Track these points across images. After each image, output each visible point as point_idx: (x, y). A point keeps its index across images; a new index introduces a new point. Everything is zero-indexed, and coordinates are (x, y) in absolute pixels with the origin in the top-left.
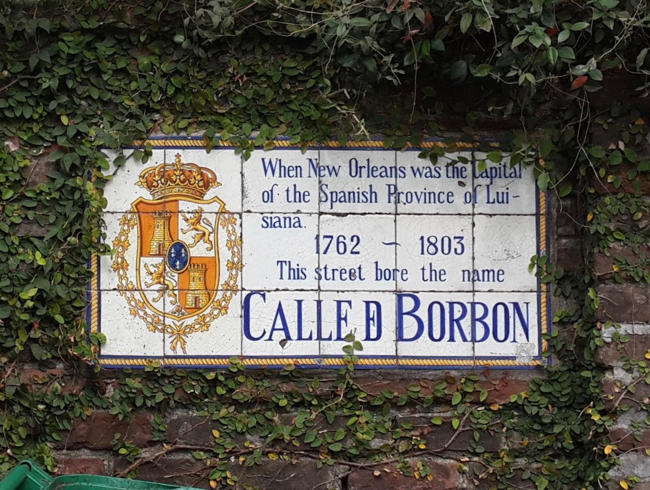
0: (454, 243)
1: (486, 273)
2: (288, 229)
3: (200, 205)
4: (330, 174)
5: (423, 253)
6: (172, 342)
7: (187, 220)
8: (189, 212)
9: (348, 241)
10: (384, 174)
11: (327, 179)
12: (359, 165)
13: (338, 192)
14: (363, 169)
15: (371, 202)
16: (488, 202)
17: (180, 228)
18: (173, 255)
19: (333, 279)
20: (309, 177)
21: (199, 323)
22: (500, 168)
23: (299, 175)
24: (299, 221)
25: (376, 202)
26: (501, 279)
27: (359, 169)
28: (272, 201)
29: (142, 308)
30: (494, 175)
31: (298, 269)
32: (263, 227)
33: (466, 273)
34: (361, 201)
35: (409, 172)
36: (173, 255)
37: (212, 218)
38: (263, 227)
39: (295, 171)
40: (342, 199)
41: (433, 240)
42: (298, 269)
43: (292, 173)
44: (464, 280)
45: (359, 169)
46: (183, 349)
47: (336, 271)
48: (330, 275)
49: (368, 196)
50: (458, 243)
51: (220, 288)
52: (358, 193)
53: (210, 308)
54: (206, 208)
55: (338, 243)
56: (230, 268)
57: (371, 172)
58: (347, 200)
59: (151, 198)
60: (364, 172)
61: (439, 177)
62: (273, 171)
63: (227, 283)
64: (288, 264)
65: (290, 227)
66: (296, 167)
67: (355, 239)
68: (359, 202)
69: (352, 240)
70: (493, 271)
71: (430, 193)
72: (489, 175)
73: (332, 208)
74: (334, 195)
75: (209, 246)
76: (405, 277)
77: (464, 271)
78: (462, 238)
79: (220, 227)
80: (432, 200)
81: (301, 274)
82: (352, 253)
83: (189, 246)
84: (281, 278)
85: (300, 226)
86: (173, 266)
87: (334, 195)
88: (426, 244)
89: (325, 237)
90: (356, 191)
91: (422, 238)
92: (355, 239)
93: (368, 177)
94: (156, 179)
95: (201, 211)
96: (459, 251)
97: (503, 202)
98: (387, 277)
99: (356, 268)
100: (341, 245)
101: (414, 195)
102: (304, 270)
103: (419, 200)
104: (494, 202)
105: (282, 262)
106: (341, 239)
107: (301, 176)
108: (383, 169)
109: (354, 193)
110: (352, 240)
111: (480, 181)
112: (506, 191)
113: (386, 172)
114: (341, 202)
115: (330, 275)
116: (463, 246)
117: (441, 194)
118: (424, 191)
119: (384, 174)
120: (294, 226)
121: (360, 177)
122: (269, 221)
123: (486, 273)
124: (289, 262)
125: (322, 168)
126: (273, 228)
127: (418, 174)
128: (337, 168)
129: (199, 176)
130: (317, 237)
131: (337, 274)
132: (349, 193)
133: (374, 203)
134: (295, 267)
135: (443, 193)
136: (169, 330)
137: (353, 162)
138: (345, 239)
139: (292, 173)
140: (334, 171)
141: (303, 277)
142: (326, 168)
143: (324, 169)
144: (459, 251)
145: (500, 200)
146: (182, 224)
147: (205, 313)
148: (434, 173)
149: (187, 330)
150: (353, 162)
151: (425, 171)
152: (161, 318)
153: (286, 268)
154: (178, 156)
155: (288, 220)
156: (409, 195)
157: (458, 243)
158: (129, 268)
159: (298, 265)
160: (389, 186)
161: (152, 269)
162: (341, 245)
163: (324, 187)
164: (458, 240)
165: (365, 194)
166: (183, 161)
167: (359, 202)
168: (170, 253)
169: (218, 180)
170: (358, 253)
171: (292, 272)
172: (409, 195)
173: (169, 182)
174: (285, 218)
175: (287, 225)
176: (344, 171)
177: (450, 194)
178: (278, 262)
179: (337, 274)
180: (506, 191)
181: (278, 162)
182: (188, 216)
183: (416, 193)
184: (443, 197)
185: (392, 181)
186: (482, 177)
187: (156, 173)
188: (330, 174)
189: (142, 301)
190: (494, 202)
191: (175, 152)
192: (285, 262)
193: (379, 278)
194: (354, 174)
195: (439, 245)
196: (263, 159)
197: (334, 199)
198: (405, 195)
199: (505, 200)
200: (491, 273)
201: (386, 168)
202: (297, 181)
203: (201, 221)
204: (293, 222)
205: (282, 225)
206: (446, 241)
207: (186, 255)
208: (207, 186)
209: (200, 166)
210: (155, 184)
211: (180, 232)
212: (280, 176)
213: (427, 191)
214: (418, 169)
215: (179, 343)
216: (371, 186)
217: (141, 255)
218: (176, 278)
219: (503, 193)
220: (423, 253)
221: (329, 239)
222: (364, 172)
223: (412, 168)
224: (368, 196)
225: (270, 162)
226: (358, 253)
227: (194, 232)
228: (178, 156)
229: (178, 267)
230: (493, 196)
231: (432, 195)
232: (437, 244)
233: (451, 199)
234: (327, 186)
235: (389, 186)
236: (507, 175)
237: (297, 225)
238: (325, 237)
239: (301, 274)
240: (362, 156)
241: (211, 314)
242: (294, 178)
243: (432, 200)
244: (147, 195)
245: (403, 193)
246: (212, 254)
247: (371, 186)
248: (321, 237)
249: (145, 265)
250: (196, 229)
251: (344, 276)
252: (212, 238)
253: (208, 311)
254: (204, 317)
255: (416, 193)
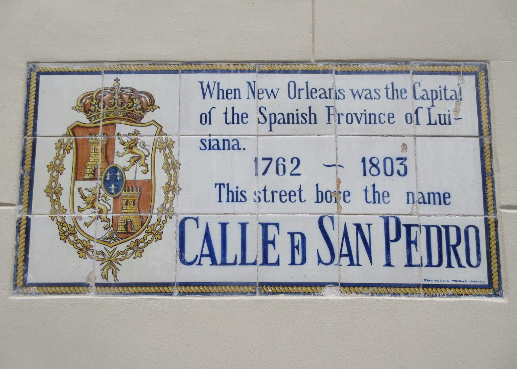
0: (397, 166)
1: (432, 195)
2: (226, 151)
3: (137, 128)
4: (269, 97)
5: (365, 175)
6: (103, 269)
7: (123, 144)
8: (125, 135)
9: (288, 163)
10: (323, 96)
11: (265, 102)
12: (297, 88)
13: (277, 114)
14: (302, 92)
15: (310, 123)
16: (430, 123)
17: (116, 152)
18: (108, 179)
19: (273, 201)
20: (248, 98)
21: (131, 248)
22: (440, 91)
23: (237, 97)
24: (238, 144)
25: (315, 123)
26: (447, 202)
27: (297, 92)
28: (210, 123)
29: (73, 234)
30: (434, 97)
31: (237, 192)
32: (201, 149)
33: (410, 195)
34: (300, 122)
35: (348, 94)
36: (108, 179)
37: (149, 141)
38: (201, 149)
39: (233, 95)
40: (281, 121)
41: (375, 161)
42: (237, 192)
43: (230, 96)
44: (408, 203)
45: (297, 92)
46: (115, 276)
47: (275, 194)
48: (269, 197)
49: (308, 118)
50: (401, 164)
51: (155, 211)
52: (297, 114)
53: (144, 233)
54: (142, 130)
55: (277, 165)
56: (167, 192)
57: (310, 95)
58: (286, 121)
59: (88, 121)
60: (303, 94)
61: (380, 97)
62: (211, 95)
63: (163, 207)
64: (226, 186)
65: (229, 149)
66: (235, 90)
67: (295, 161)
68: (298, 123)
69: (292, 162)
70: (439, 194)
71: (370, 115)
72: (430, 97)
73: (271, 130)
74: (273, 116)
75: (144, 168)
76: (347, 199)
77: (408, 193)
78: (406, 159)
79: (157, 150)
80: (373, 122)
81: (240, 197)
82: (291, 174)
83: (125, 169)
84: (220, 201)
85: (239, 149)
86: (108, 190)
87: (273, 116)
88: (368, 165)
89: (263, 159)
90: (295, 113)
91: (364, 160)
92: (295, 161)
93: (308, 98)
94: (94, 104)
95: (137, 133)
96: (402, 172)
97: (445, 123)
98: (329, 200)
99: (296, 190)
100: (281, 168)
101: (354, 116)
102: (243, 193)
103: (359, 122)
104: (436, 124)
105: (220, 185)
106: (281, 161)
107: (240, 98)
108: (322, 91)
109: (293, 115)
110: (292, 162)
111: (419, 103)
112: (448, 113)
113: (325, 95)
114: (279, 123)
115: (269, 197)
116: (406, 168)
117: (382, 115)
118: (365, 113)
119: (323, 96)
120: (233, 148)
121: (300, 98)
122: (207, 144)
123: (432, 195)
124: (228, 185)
125: (260, 91)
126: (212, 151)
127: (357, 97)
128: (275, 92)
129: (137, 100)
130: (256, 160)
131: (277, 196)
132: (288, 114)
133: (313, 125)
134: (234, 190)
135: (384, 114)
136: (101, 256)
137: (292, 85)
138: (284, 161)
139: (230, 96)
140: (273, 94)
141: (243, 199)
142: (265, 91)
143: (263, 93)
144: (402, 172)
145: (443, 122)
146: (119, 148)
147: (138, 237)
148: (374, 94)
149: (120, 256)
150: (292, 85)
151: (365, 93)
152: (92, 243)
153: (224, 191)
154: (117, 80)
155: (226, 142)
156: (349, 116)
157: (401, 164)
158: (63, 192)
159: (237, 188)
160: (328, 108)
161: (86, 193)
162: (281, 168)
163: (263, 110)
164: (401, 161)
165: (304, 115)
166: (123, 84)
167: (298, 123)
168: (106, 177)
169: (156, 104)
170: (299, 175)
171: (230, 194)
172: (349, 116)
173: (107, 106)
174: (224, 140)
175: (226, 147)
176: (283, 94)
177: (391, 116)
178: (216, 185)
179: (277, 196)
180: (447, 113)
181: (216, 85)
182: (125, 139)
183: (356, 114)
184: (384, 118)
185: (330, 102)
186: (423, 99)
187: (94, 96)
188: (269, 97)
189: (73, 225)
190: (436, 124)
191: (115, 76)
192: (223, 184)
193: (320, 200)
194: (292, 95)
195: (381, 166)
196: (201, 83)
197: (273, 121)
198: (345, 116)
199: (447, 122)
200: (437, 196)
201: (324, 91)
202: (235, 103)
203: (138, 145)
204: (232, 144)
205: (221, 147)
206: (388, 162)
207: (122, 177)
208: (144, 110)
209: (138, 91)
210: (92, 108)
211: (116, 157)
212: (218, 98)
213: (367, 113)
214: (358, 91)
215: (110, 271)
216: (310, 108)
217: (76, 179)
218: (111, 202)
219: (445, 115)
220: (365, 175)
221: (269, 161)
222: (303, 94)
223: (352, 90)
224: (308, 118)
225: (208, 86)
226: (299, 175)
227: (131, 155)
228: (117, 80)
229: (113, 191)
230: (434, 118)
231: (372, 116)
232: (378, 165)
233: (392, 120)
234: (265, 109)
235: (328, 108)
236: (448, 97)
237: (236, 147)
238: (263, 159)
239: (240, 197)
240: (301, 80)
241: (144, 239)
242: (232, 99)
243: (373, 122)
244: (83, 118)
245: (343, 115)
246: (148, 177)
247: (310, 108)
248: (260, 160)
249: (80, 189)
250: (133, 153)
251: (284, 199)
252: (148, 161)
253: (140, 237)
254: (137, 242)
255: (356, 114)
